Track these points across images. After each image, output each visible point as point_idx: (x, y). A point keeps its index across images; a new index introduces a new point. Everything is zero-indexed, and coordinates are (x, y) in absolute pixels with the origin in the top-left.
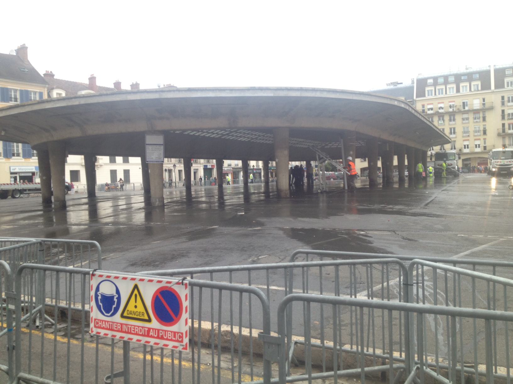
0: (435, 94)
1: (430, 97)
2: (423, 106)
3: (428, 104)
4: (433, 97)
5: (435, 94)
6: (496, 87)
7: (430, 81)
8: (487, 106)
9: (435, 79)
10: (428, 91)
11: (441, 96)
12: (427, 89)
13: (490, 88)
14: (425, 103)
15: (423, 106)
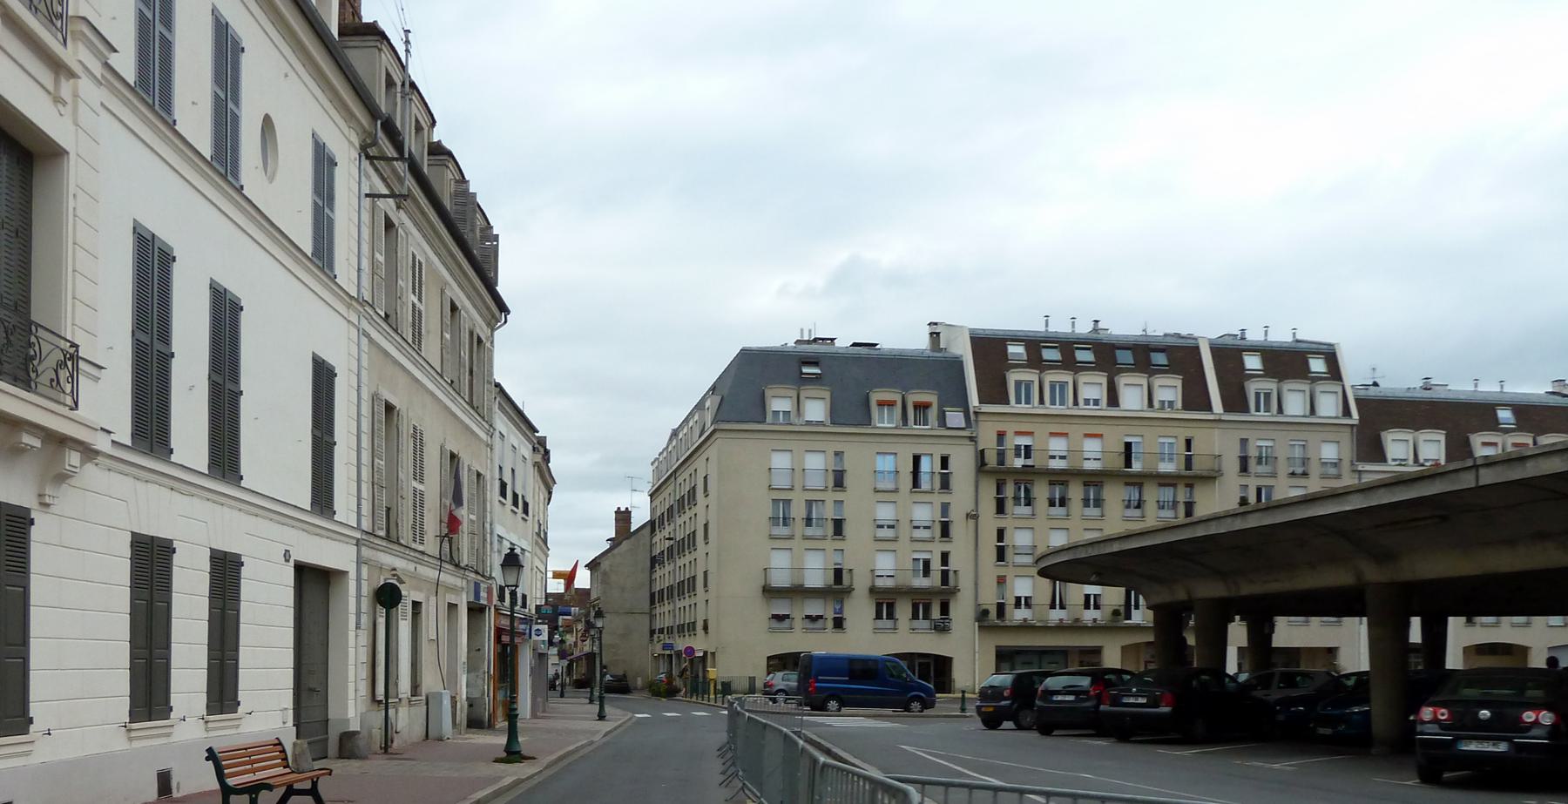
0: (1042, 401)
1: (1023, 408)
2: (1001, 436)
3: (1018, 433)
4: (1035, 408)
5: (1042, 401)
6: (1229, 406)
7: (1016, 350)
8: (1199, 466)
9: (1035, 344)
10: (1018, 384)
11: (1057, 409)
12: (1013, 377)
13: (1209, 408)
14: (1010, 427)
15: (1001, 436)
